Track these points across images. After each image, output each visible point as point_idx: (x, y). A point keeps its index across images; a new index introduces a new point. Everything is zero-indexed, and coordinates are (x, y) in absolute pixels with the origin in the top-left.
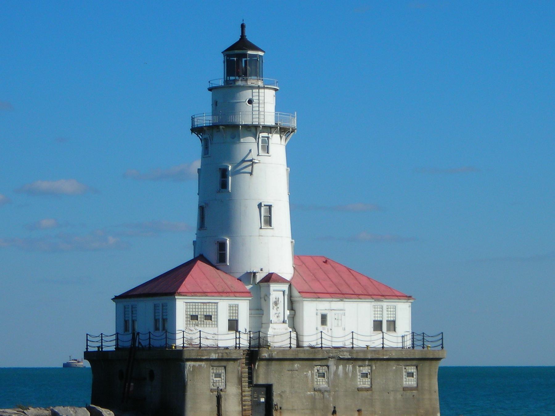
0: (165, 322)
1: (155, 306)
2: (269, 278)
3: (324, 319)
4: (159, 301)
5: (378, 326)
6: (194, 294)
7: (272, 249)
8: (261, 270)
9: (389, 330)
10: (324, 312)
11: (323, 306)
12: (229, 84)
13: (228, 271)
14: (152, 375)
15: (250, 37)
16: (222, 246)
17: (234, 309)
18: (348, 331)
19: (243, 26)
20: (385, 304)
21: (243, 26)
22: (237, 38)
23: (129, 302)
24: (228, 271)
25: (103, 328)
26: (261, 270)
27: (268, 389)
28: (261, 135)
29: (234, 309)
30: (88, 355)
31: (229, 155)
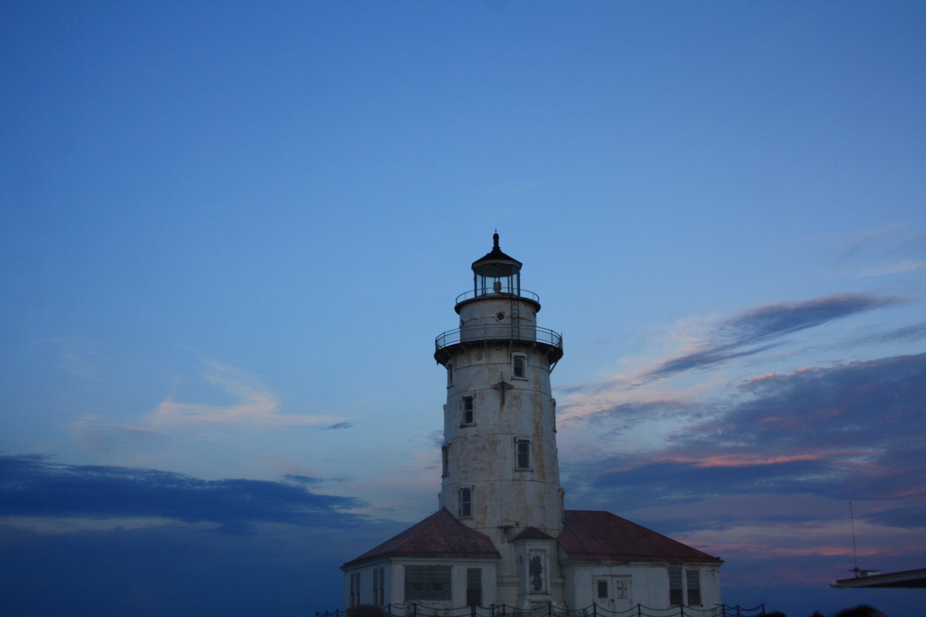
3: (603, 590)
5: (675, 597)
6: (417, 554)
8: (517, 524)
9: (690, 603)
10: (602, 579)
11: (602, 571)
17: (474, 577)
18: (635, 604)
19: (496, 237)
20: (684, 569)
21: (496, 237)
22: (489, 249)
26: (517, 524)
28: (514, 354)
29: (474, 577)
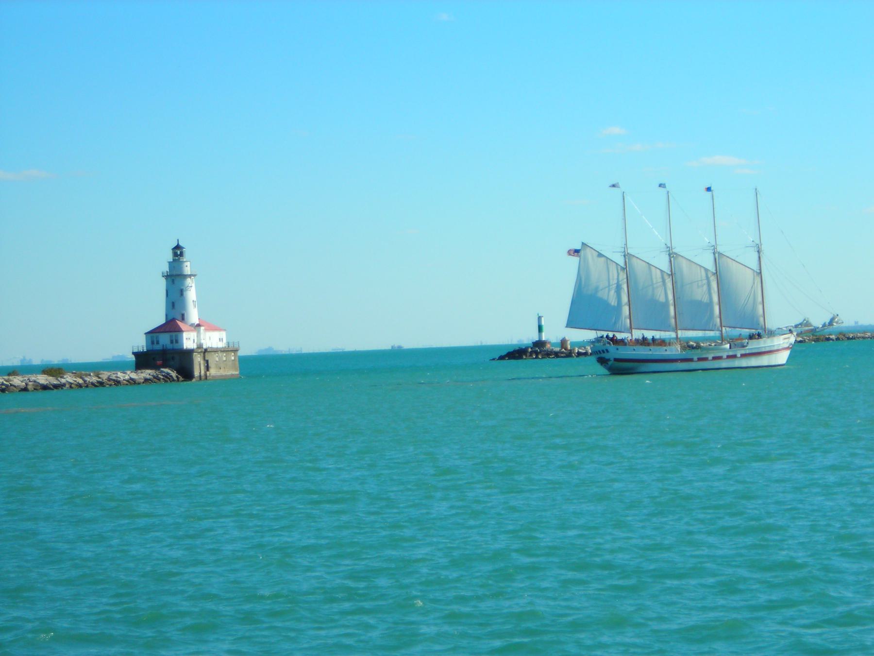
0: (177, 341)
1: (171, 336)
2: (199, 325)
4: (174, 334)
7: (194, 316)
12: (174, 260)
13: (186, 323)
14: (173, 358)
15: (180, 244)
16: (183, 315)
23: (154, 335)
24: (186, 323)
25: (141, 344)
27: (207, 362)
30: (133, 353)
31: (183, 284)
